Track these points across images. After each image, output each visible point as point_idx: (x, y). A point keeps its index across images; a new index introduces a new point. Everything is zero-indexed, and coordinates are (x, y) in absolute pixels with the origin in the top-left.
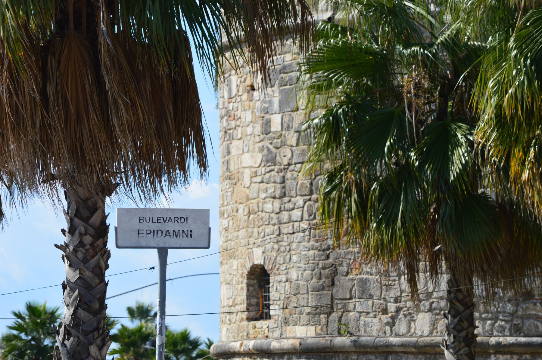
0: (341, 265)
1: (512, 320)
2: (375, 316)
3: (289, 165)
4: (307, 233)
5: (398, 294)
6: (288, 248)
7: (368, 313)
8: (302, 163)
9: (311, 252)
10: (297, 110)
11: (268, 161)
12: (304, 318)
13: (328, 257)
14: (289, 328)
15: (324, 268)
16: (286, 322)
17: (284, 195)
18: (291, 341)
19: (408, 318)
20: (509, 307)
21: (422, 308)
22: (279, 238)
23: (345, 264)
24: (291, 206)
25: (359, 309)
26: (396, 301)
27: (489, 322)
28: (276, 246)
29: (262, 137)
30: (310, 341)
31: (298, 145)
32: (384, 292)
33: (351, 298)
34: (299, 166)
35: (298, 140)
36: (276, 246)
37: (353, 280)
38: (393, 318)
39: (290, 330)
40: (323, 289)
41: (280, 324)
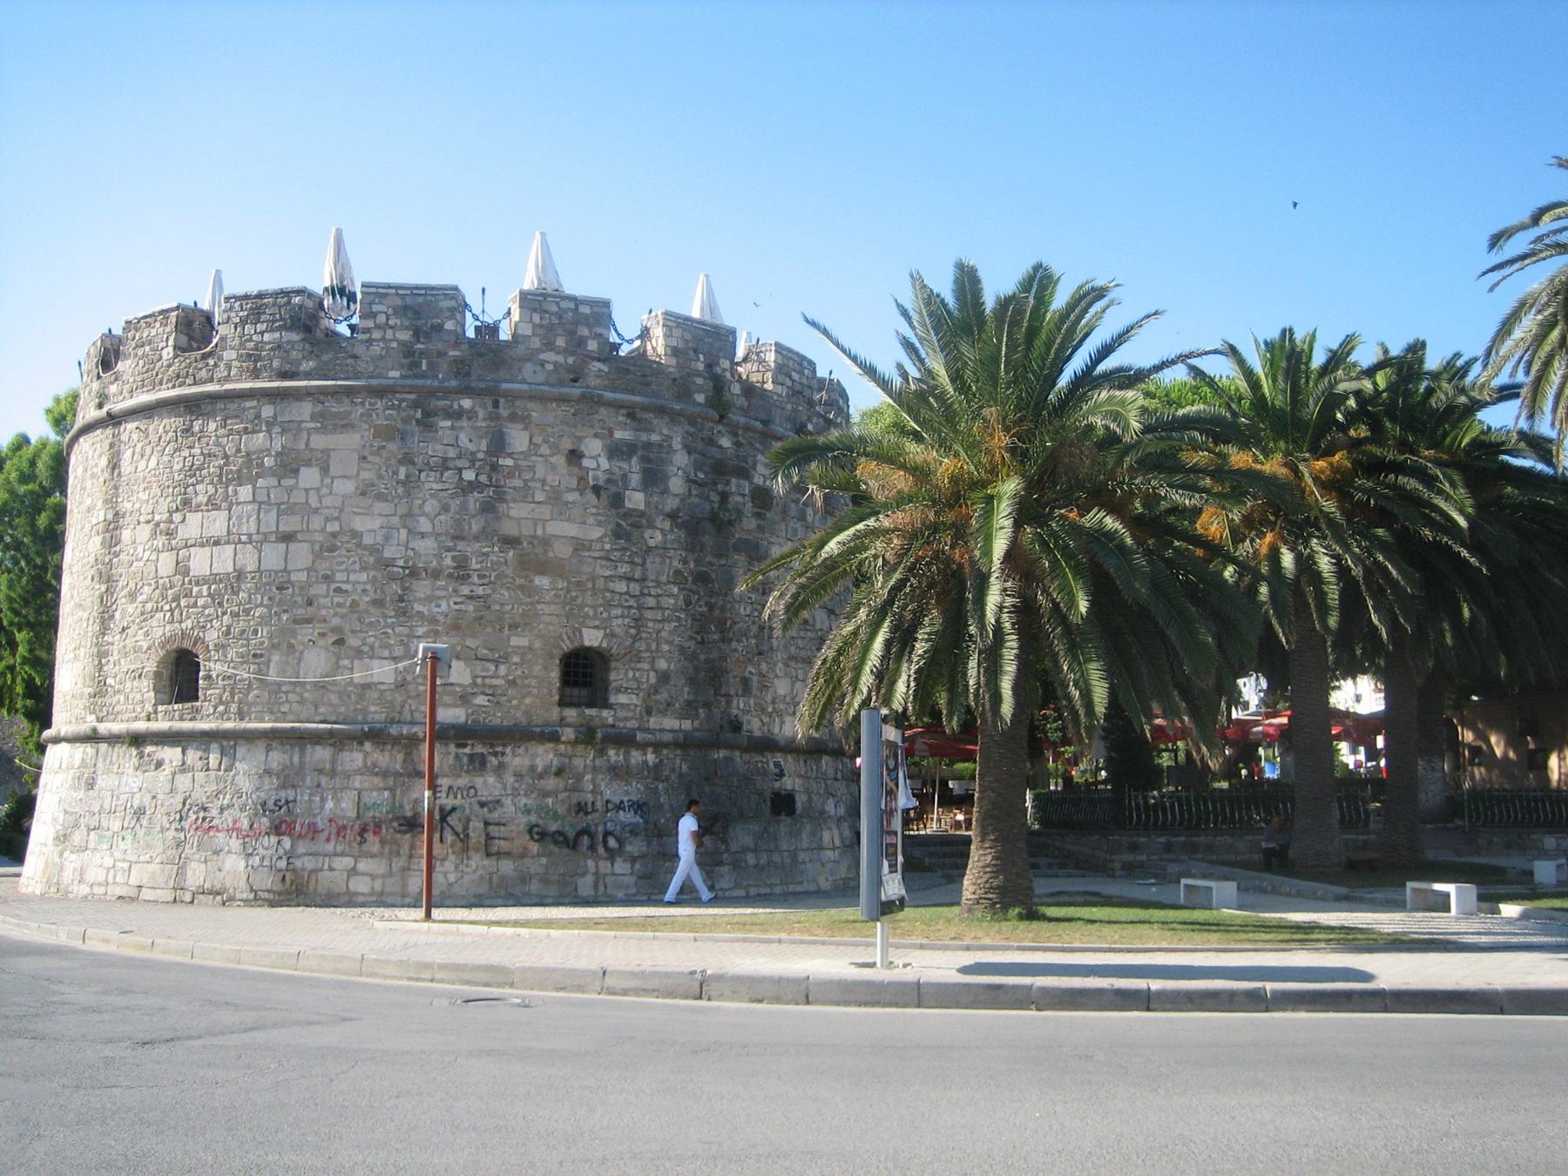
14: (652, 720)
28: (633, 631)
39: (653, 722)
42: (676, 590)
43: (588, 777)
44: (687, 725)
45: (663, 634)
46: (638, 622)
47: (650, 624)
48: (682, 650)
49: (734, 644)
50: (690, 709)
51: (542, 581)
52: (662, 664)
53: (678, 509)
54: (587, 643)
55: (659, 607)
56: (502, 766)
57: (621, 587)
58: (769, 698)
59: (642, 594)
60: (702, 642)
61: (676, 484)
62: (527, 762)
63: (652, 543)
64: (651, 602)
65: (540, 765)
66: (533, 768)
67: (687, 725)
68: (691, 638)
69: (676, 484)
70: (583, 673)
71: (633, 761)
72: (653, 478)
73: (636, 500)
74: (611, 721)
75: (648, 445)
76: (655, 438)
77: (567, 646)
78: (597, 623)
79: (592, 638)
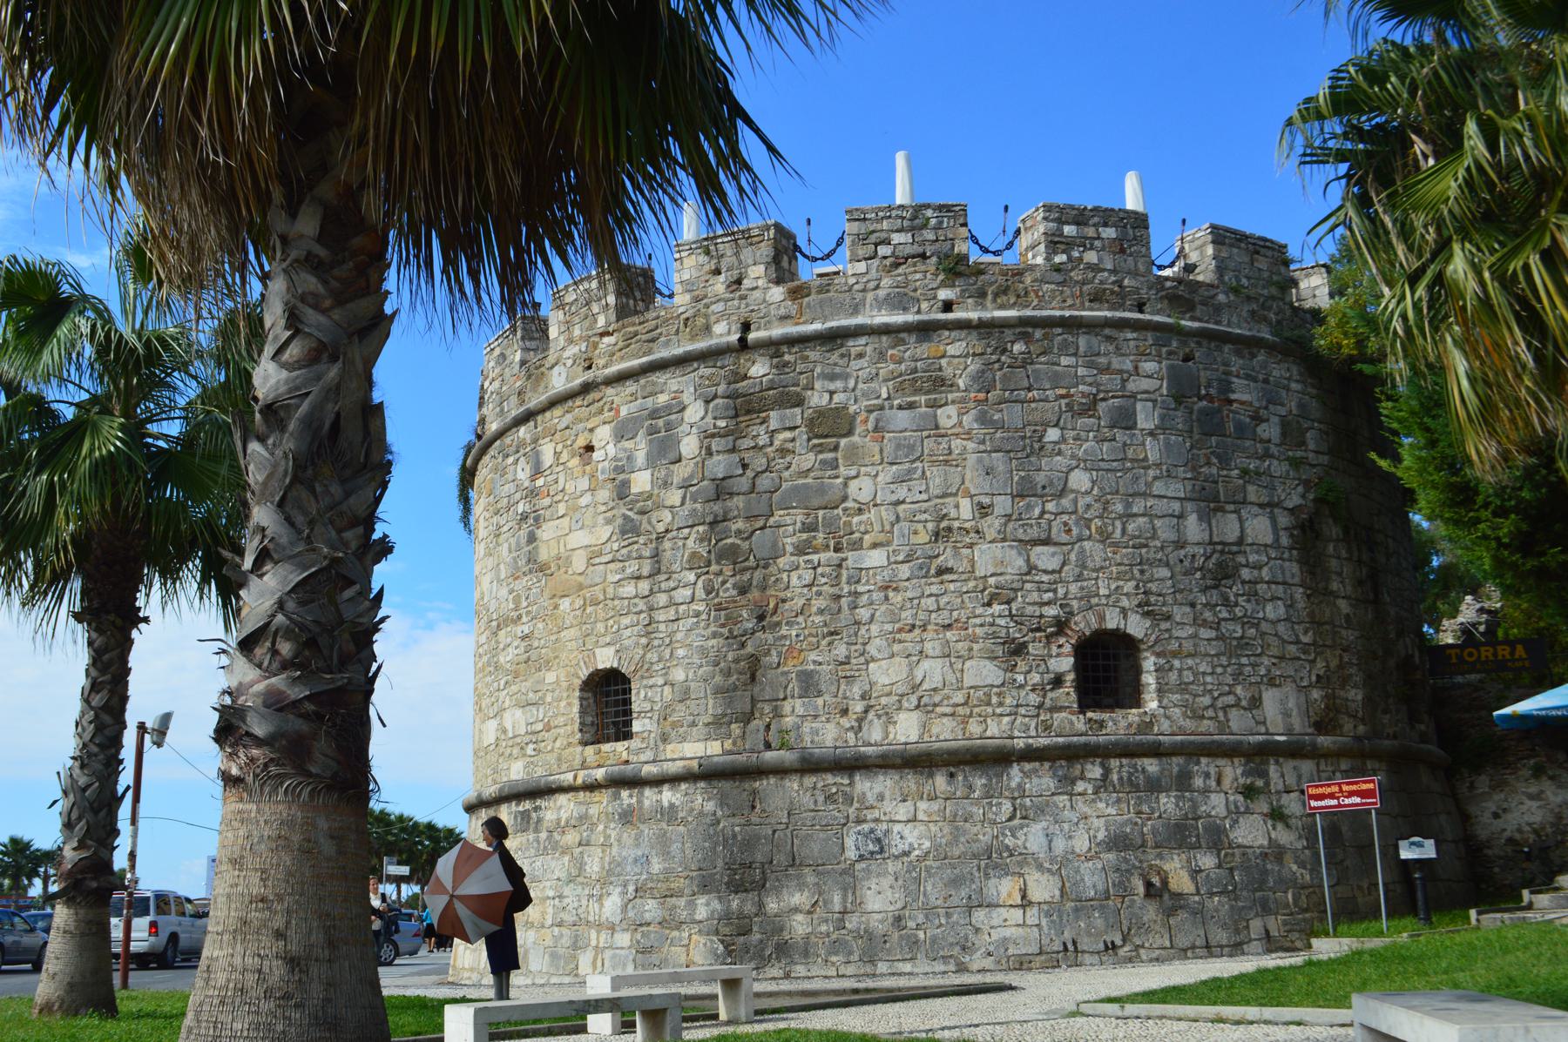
0: (768, 653)
1: (1038, 715)
2: (828, 721)
3: (667, 531)
4: (704, 617)
5: (867, 687)
6: (667, 641)
7: (816, 717)
8: (692, 526)
9: (713, 642)
10: (680, 460)
11: (623, 532)
12: (700, 730)
13: (743, 645)
14: (669, 747)
15: (736, 661)
16: (665, 738)
17: (659, 572)
18: (680, 764)
19: (884, 718)
20: (1034, 699)
21: (906, 704)
22: (650, 629)
23: (774, 653)
24: (672, 584)
25: (800, 710)
26: (863, 698)
27: (1006, 720)
28: (644, 641)
29: (612, 504)
30: (716, 759)
31: (683, 504)
32: (843, 687)
33: (785, 699)
34: (686, 531)
35: (684, 498)
36: (644, 641)
37: (786, 673)
38: (860, 720)
39: (671, 750)
40: (735, 688)
41: (652, 742)
42: (691, 577)
43: (601, 827)
44: (714, 748)
45: (679, 636)
46: (649, 628)
47: (662, 627)
48: (703, 651)
49: (784, 631)
50: (718, 725)
51: (565, 604)
52: (679, 675)
53: (691, 477)
54: (600, 666)
55: (672, 603)
56: (539, 820)
57: (629, 589)
58: (856, 690)
59: (652, 592)
60: (731, 636)
61: (689, 446)
62: (554, 817)
63: (661, 528)
64: (662, 599)
65: (564, 815)
66: (559, 820)
67: (714, 748)
68: (715, 635)
69: (689, 446)
70: (607, 703)
71: (647, 803)
72: (664, 451)
73: (641, 481)
74: (625, 756)
75: (654, 414)
76: (662, 399)
77: (584, 673)
78: (608, 640)
79: (605, 659)
